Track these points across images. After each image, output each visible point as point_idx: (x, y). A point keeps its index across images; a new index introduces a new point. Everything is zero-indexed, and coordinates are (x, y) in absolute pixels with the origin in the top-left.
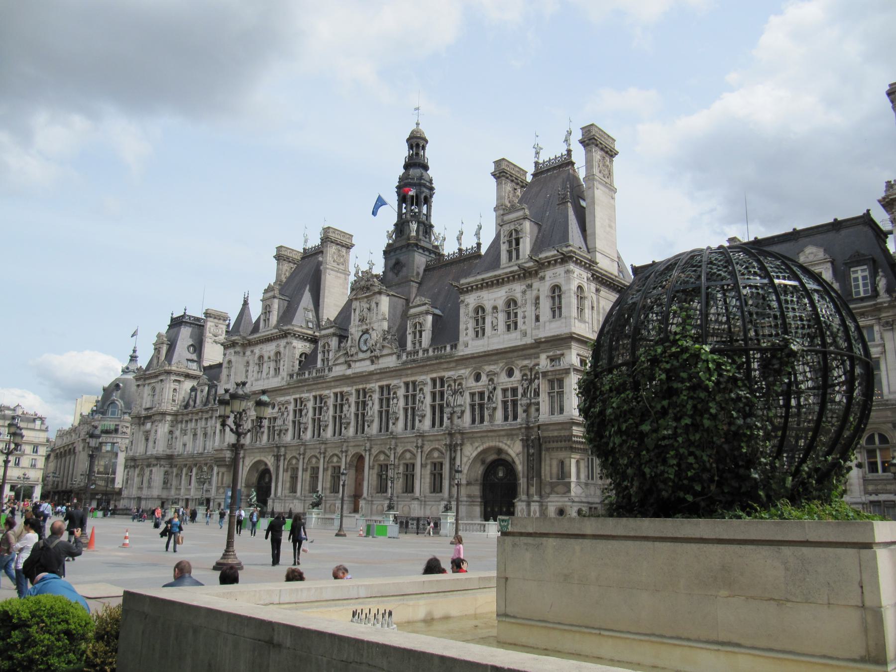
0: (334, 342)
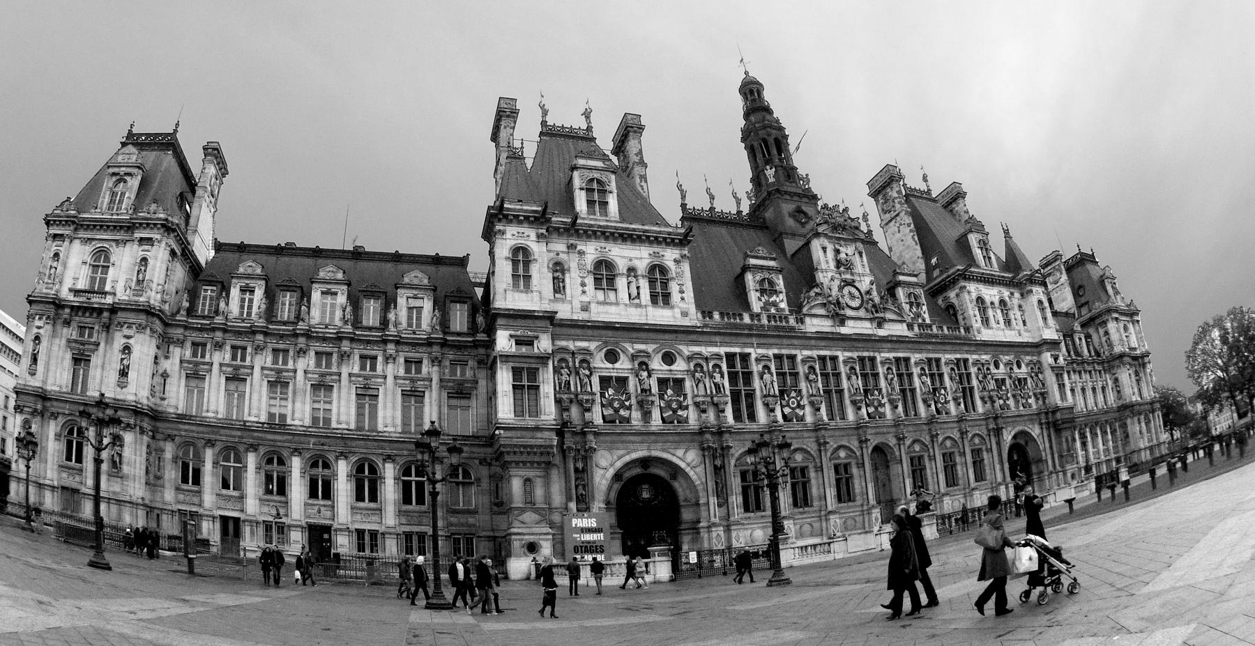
0: (780, 282)
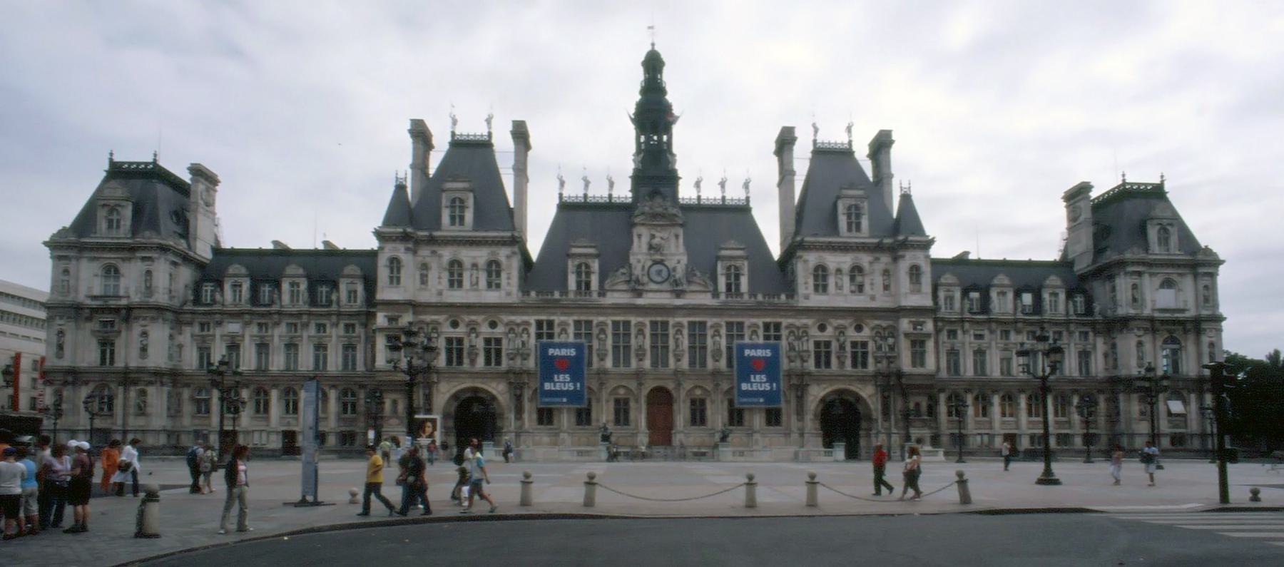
0: (595, 265)
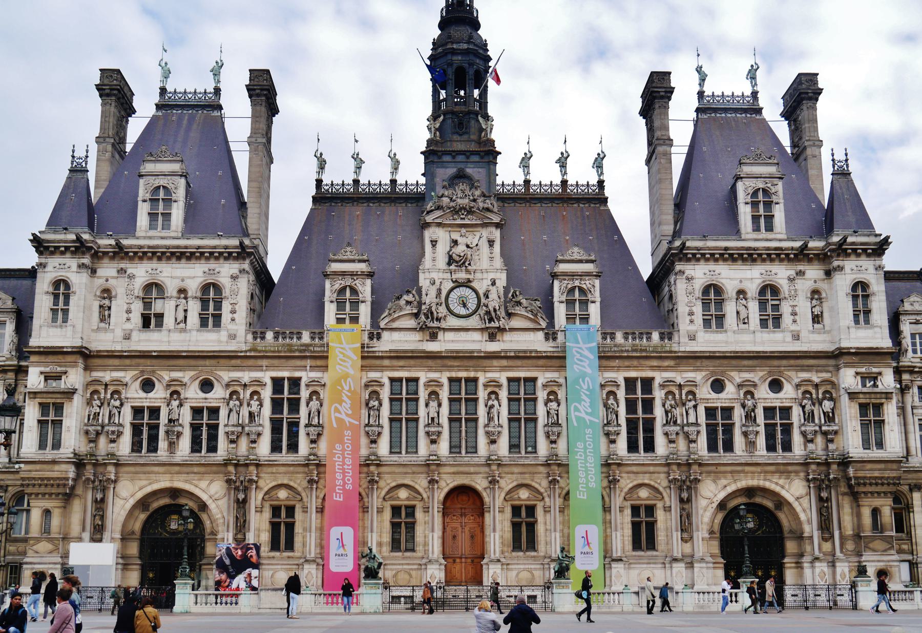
0: (365, 289)
